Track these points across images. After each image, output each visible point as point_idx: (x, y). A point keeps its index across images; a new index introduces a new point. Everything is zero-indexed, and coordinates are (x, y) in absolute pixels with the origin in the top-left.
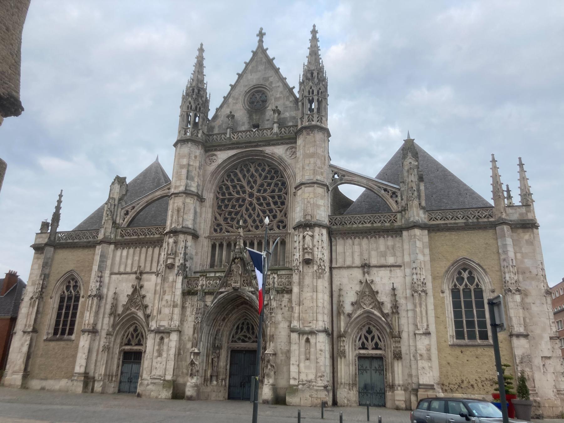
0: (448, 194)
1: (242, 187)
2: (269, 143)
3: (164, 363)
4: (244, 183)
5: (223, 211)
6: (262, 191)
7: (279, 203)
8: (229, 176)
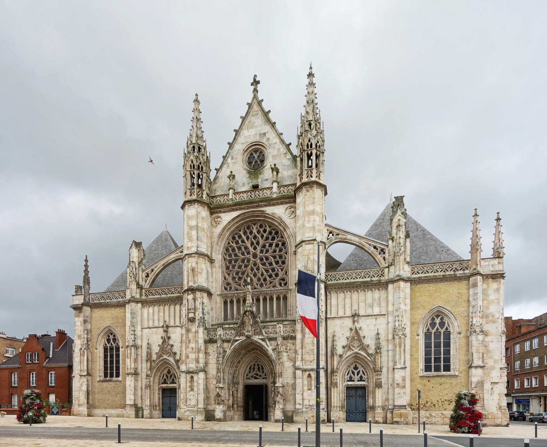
1: (246, 248)
2: (270, 202)
3: (196, 395)
4: (248, 244)
6: (264, 252)
7: (280, 263)
8: (234, 238)
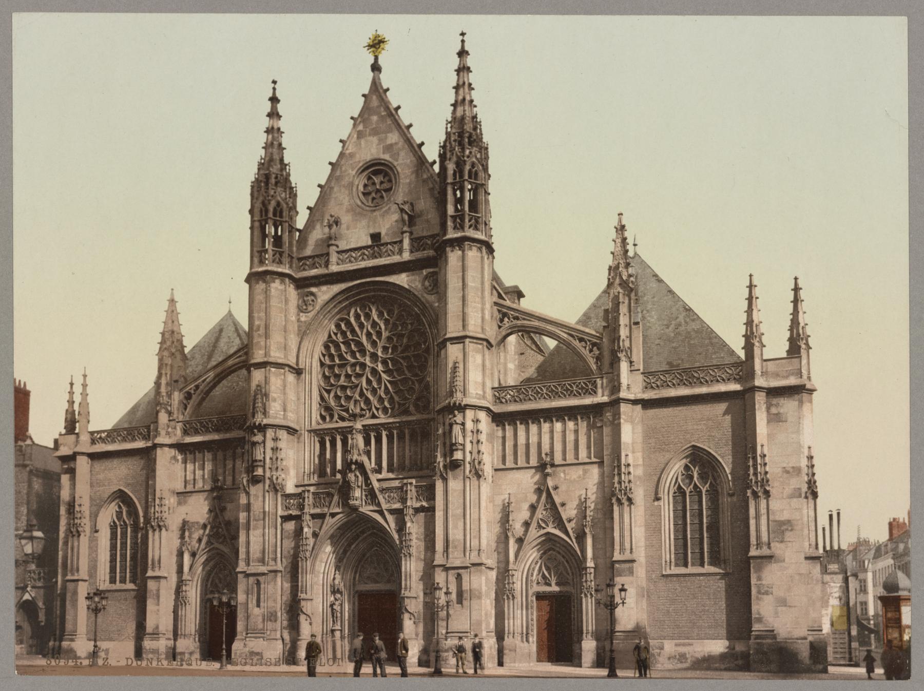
1: (359, 344)
4: (364, 340)
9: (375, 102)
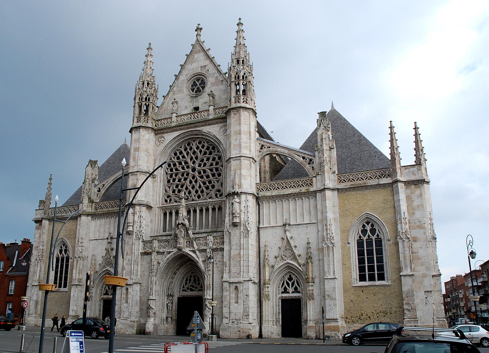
0: (360, 157)
1: (186, 163)
4: (189, 161)
5: (171, 184)
6: (202, 165)
7: (216, 175)
8: (175, 154)
9: (198, 48)
